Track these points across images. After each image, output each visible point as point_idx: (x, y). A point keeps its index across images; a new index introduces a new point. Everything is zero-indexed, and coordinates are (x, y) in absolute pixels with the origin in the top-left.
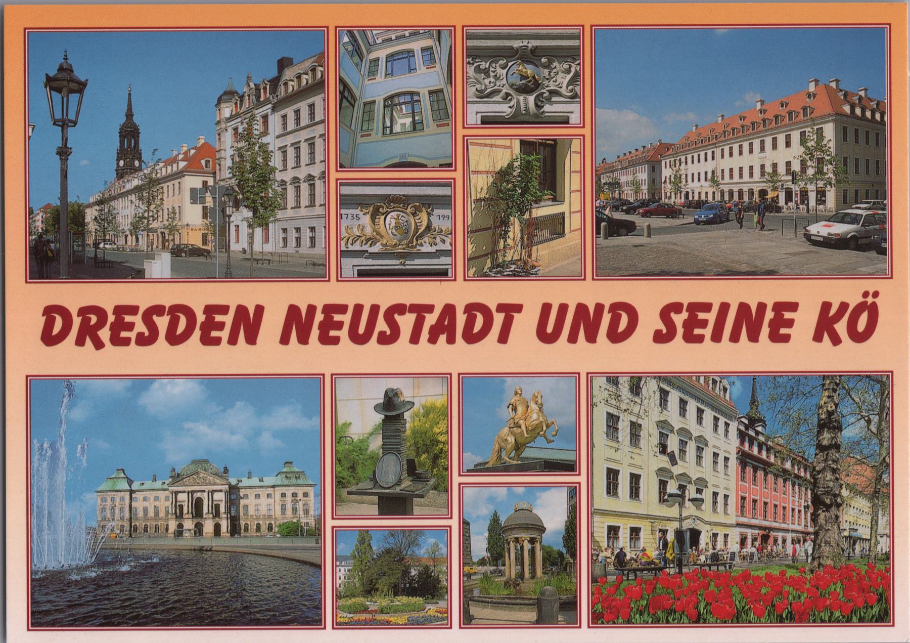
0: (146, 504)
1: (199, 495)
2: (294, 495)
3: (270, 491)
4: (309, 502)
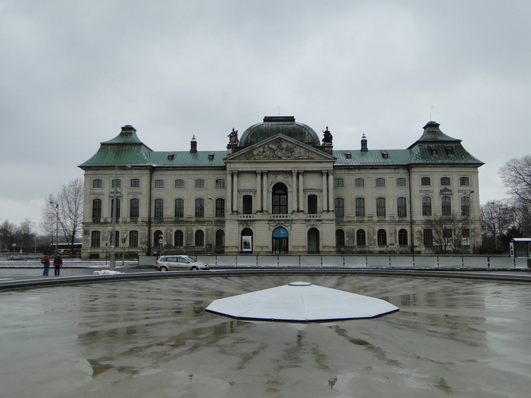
0: (180, 193)
1: (280, 179)
2: (445, 181)
3: (402, 174)
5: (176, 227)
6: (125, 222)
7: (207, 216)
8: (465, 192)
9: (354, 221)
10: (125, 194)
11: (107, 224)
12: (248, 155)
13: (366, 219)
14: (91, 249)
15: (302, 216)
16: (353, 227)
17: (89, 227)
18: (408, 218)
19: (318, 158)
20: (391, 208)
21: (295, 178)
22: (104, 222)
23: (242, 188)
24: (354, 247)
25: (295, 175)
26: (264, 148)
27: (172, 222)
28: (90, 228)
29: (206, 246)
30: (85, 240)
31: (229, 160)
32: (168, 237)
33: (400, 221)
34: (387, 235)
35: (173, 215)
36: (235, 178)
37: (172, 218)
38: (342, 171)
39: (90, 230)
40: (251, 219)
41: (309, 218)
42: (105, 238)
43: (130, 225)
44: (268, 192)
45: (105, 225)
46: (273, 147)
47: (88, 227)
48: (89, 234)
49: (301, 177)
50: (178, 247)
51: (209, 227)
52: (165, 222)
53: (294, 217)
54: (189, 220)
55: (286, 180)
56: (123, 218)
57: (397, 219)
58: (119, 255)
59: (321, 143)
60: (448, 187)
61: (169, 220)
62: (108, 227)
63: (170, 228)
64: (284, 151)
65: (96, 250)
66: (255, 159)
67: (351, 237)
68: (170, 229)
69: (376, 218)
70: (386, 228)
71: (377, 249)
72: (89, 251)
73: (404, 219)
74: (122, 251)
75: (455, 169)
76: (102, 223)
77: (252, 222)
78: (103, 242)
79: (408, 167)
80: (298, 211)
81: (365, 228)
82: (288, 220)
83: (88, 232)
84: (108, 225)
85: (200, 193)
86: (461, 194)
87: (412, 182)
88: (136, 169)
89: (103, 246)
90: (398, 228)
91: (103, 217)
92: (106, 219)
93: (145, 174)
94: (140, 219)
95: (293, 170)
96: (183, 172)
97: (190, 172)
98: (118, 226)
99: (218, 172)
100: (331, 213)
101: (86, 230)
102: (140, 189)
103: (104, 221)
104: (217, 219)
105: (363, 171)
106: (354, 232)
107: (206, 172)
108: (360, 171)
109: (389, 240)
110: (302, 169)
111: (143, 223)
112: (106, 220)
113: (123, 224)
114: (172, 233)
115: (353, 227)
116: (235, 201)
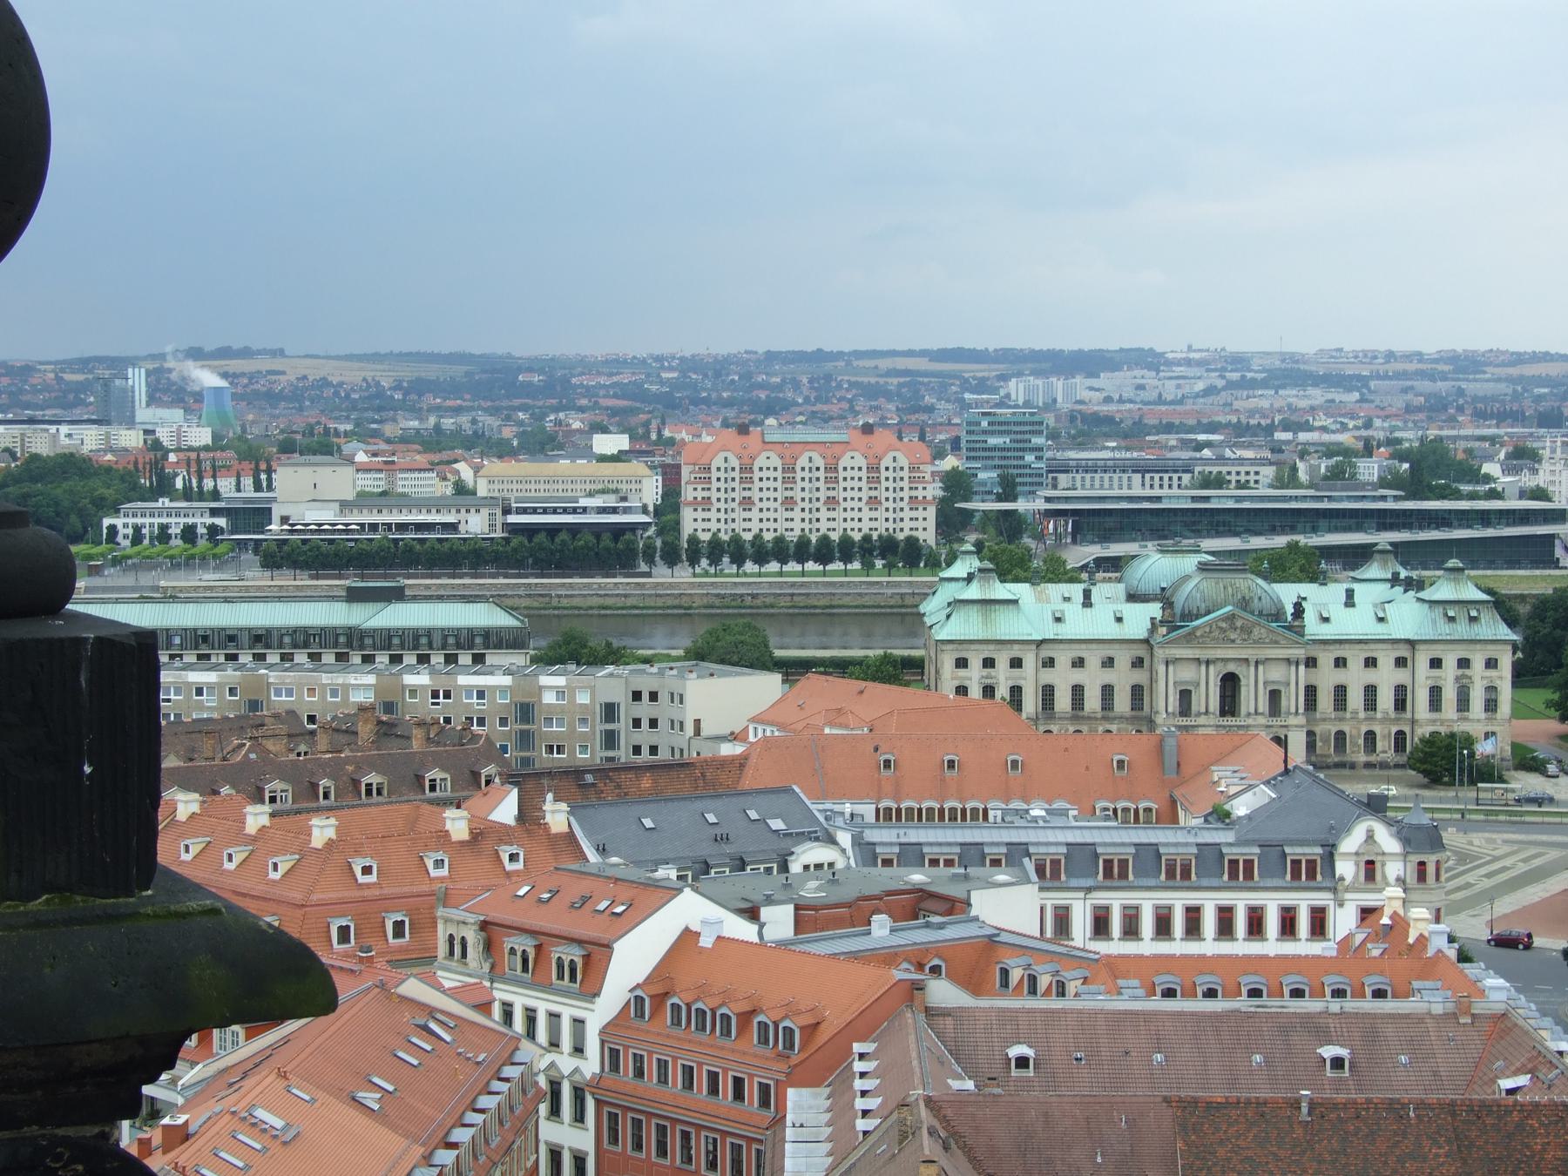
1: (1231, 668)
2: (1464, 663)
4: (1498, 682)
8: (1491, 679)
9: (1331, 719)
10: (1002, 678)
13: (1348, 715)
15: (1262, 720)
16: (1330, 727)
18: (1408, 715)
19: (1284, 642)
20: (1386, 700)
21: (1252, 669)
23: (1178, 679)
24: (1330, 756)
25: (1253, 664)
33: (1397, 720)
34: (1378, 738)
35: (1069, 708)
36: (1171, 668)
38: (1317, 646)
40: (1193, 723)
41: (1270, 723)
44: (1215, 685)
46: (1224, 625)
49: (1261, 668)
51: (1122, 726)
53: (1250, 721)
54: (1093, 715)
55: (1239, 668)
57: (1392, 714)
59: (1289, 618)
60: (1467, 672)
61: (1063, 715)
64: (1238, 631)
66: (1199, 643)
67: (1326, 741)
69: (1362, 715)
70: (1377, 729)
71: (1362, 758)
73: (1403, 715)
75: (1478, 647)
79: (1412, 644)
80: (1256, 713)
81: (1346, 729)
82: (1243, 726)
85: (1108, 677)
86: (1485, 682)
87: (1416, 664)
90: (1394, 729)
94: (1024, 715)
95: (1250, 657)
96: (1083, 646)
97: (1094, 646)
100: (1300, 717)
105: (1347, 646)
106: (1330, 735)
107: (1117, 646)
108: (1342, 646)
109: (1380, 745)
110: (1263, 657)
115: (1330, 727)
116: (1171, 699)
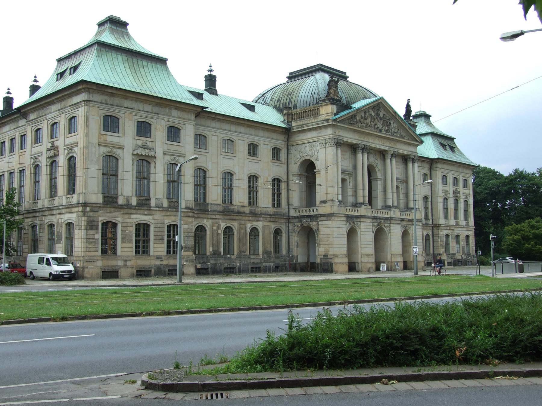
5: (225, 221)
6: (160, 207)
7: (263, 206)
11: (131, 209)
12: (351, 120)
14: (102, 260)
17: (95, 215)
22: (124, 205)
26: (365, 113)
27: (219, 212)
28: (98, 217)
29: (263, 254)
30: (91, 241)
31: (338, 122)
32: (215, 238)
37: (220, 205)
39: (100, 219)
42: (127, 238)
43: (168, 213)
45: (126, 211)
47: (96, 213)
48: (97, 229)
50: (229, 256)
52: (211, 211)
54: (241, 210)
56: (156, 199)
58: (153, 270)
62: (133, 216)
63: (217, 223)
65: (112, 263)
68: (217, 225)
72: (99, 263)
74: (158, 263)
76: (122, 207)
77: (339, 218)
78: (124, 245)
83: (95, 223)
84: (132, 211)
88: (177, 108)
89: (123, 254)
91: (122, 195)
92: (128, 199)
93: (191, 120)
97: (242, 129)
98: (149, 214)
99: (274, 135)
101: (91, 219)
102: (183, 148)
103: (125, 203)
104: (275, 212)
111: (189, 211)
112: (128, 200)
113: (159, 210)
114: (220, 231)
